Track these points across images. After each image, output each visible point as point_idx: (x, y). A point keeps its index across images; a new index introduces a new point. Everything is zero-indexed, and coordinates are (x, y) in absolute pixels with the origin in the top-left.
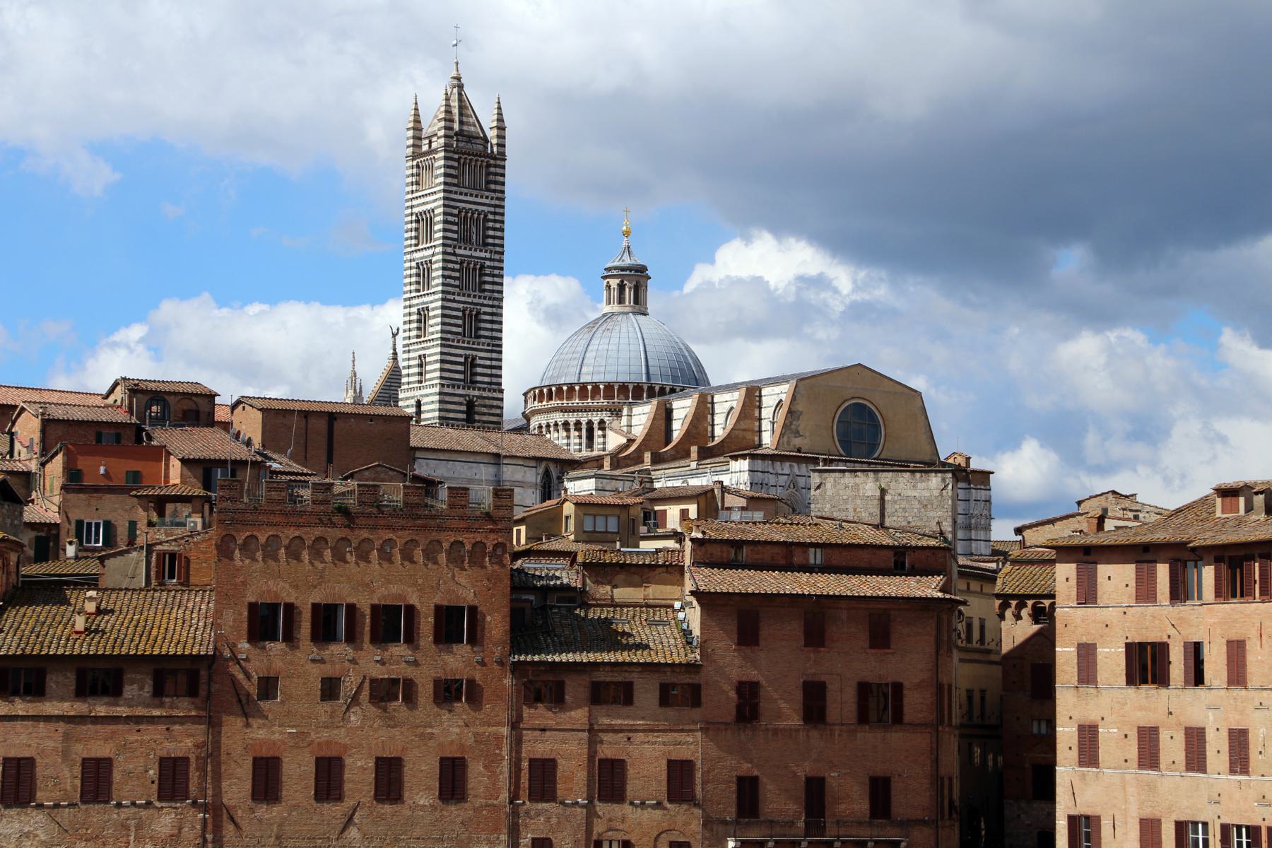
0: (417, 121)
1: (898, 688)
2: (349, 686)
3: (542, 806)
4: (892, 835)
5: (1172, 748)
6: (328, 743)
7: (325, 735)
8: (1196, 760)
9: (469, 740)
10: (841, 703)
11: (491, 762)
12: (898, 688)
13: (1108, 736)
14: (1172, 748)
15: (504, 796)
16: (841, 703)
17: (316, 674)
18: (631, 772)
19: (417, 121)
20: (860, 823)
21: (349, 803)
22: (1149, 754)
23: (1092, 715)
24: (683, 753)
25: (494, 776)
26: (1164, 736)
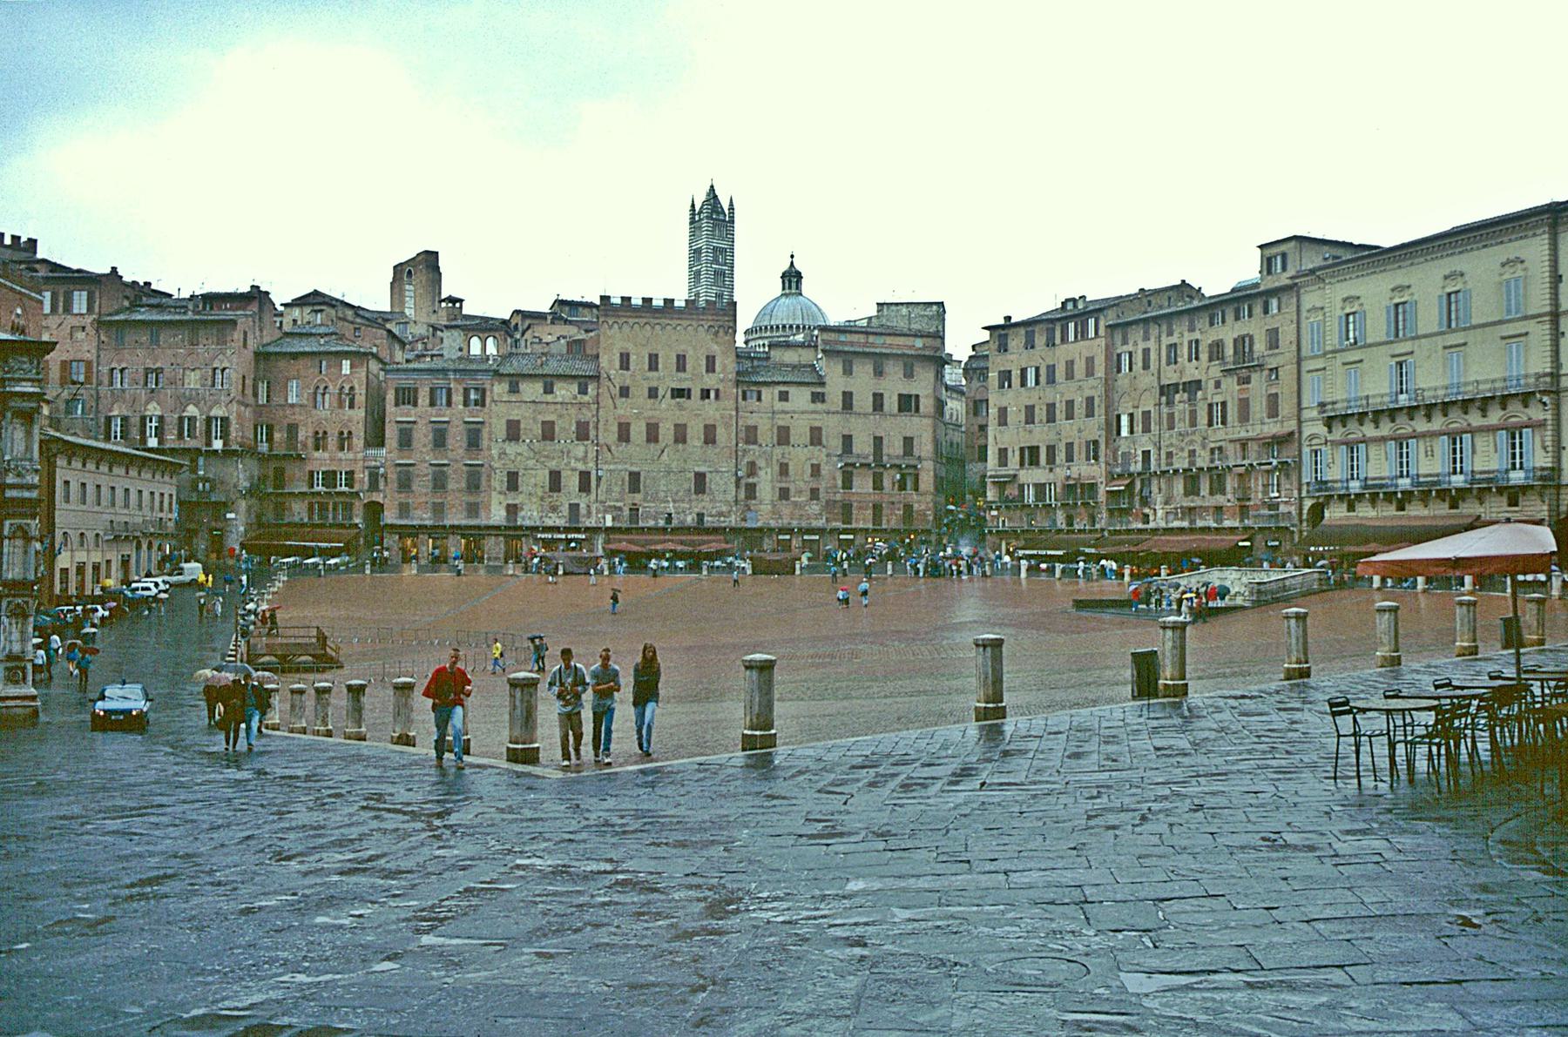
0: (693, 206)
1: (917, 396)
2: (661, 392)
3: (751, 447)
4: (913, 462)
5: (1040, 413)
6: (653, 417)
7: (650, 413)
8: (1051, 418)
9: (718, 417)
10: (891, 403)
11: (727, 426)
12: (917, 396)
13: (1012, 410)
14: (1040, 413)
15: (734, 442)
16: (891, 403)
17: (646, 385)
18: (792, 432)
19: (693, 206)
20: (898, 457)
21: (662, 444)
22: (1030, 419)
23: (1004, 404)
24: (817, 424)
25: (729, 434)
26: (1037, 410)
